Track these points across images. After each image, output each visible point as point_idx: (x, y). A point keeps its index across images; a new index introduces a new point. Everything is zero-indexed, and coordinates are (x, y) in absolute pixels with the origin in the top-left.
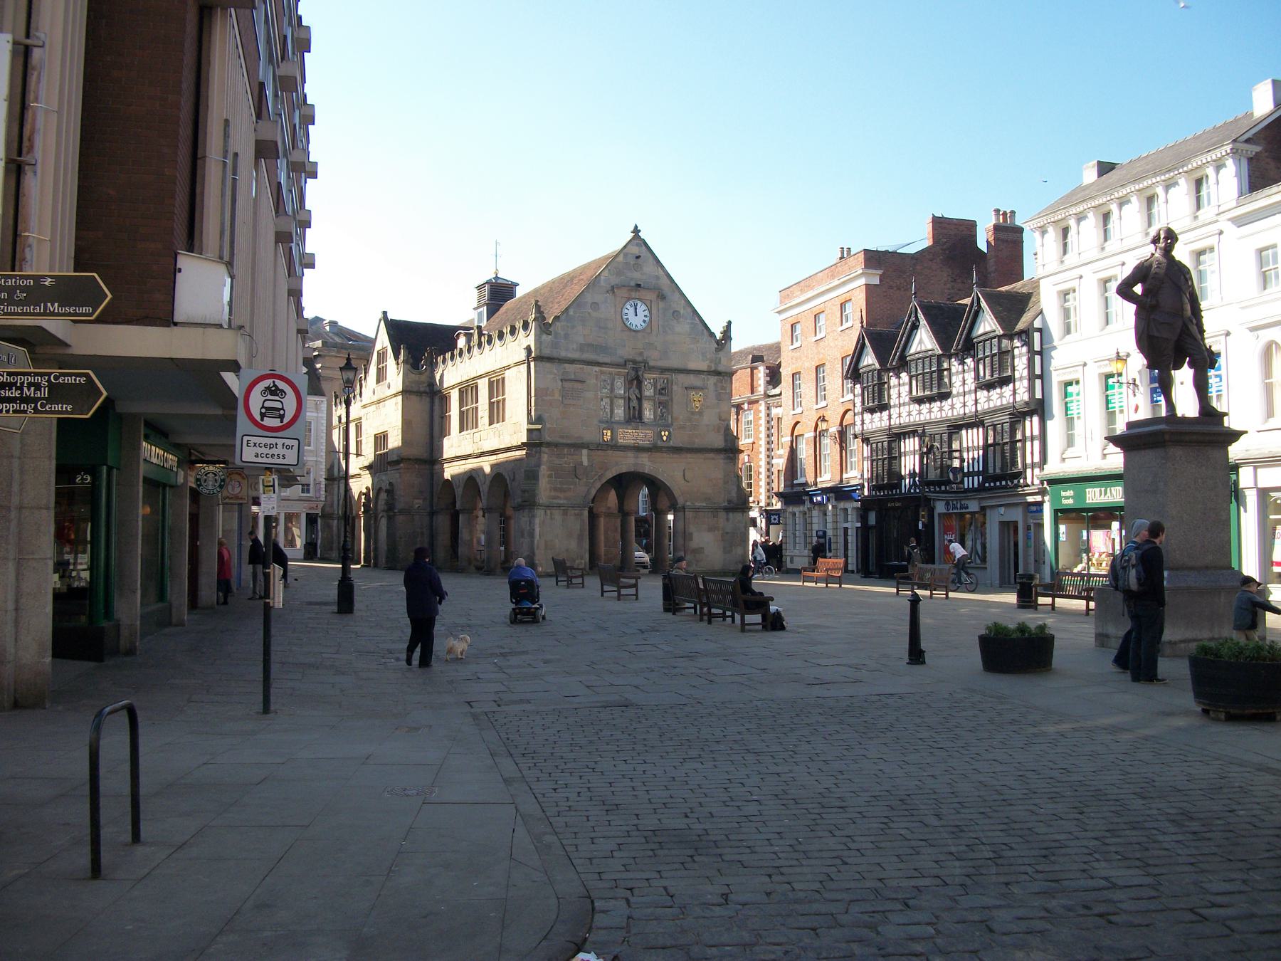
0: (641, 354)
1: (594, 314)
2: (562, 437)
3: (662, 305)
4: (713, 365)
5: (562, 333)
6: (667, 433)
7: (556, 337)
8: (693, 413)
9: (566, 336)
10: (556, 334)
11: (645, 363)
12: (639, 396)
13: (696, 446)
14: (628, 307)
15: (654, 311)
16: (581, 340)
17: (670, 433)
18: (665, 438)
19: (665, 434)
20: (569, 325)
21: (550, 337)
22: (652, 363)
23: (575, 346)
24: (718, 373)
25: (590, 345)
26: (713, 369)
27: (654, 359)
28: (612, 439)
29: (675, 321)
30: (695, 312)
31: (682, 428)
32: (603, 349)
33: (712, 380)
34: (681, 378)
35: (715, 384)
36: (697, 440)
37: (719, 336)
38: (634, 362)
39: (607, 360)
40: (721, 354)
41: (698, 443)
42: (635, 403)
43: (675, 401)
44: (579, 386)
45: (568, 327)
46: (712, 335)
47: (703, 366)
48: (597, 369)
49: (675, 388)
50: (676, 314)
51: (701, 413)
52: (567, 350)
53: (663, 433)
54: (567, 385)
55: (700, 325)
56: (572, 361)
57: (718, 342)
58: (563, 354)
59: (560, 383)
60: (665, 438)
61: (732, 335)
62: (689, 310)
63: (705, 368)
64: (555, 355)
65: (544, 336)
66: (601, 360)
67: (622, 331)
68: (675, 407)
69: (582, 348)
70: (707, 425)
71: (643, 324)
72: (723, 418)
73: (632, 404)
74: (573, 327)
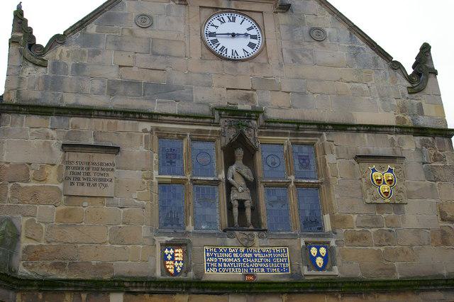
0: (247, 98)
1: (141, 33)
2: (59, 266)
3: (283, 18)
4: (408, 118)
5: (70, 63)
6: (323, 250)
7: (54, 70)
8: (379, 206)
9: (79, 69)
10: (56, 65)
11: (256, 113)
12: (250, 178)
13: (398, 276)
14: (216, 22)
15: (270, 27)
16: (113, 74)
17: (330, 251)
18: (319, 261)
19: (317, 252)
20: (86, 50)
21: (43, 69)
22: (272, 114)
23: (97, 85)
24: (420, 131)
25: (131, 83)
26: (409, 123)
27: (276, 106)
28: (186, 270)
29: (316, 43)
30: (354, 29)
31: (353, 239)
32: (165, 90)
33: (410, 144)
34: (342, 138)
35: (420, 151)
36: (396, 264)
37: (410, 71)
38: (232, 112)
39: (173, 108)
40: (423, 99)
41: (400, 269)
42: (241, 193)
43: (334, 181)
44: (106, 158)
45: (84, 53)
46: (397, 66)
47: (389, 119)
48: (148, 126)
49: (330, 158)
50: (317, 35)
51: (398, 206)
52: (79, 92)
53: (314, 251)
54: (74, 157)
55: (369, 52)
56: (86, 112)
57: (409, 78)
58: (70, 99)
59: (59, 154)
60: (319, 261)
61: (437, 65)
62: (343, 27)
63: (392, 122)
64: (50, 99)
65: (30, 68)
66: (156, 108)
67: (202, 59)
68: (336, 196)
69: (112, 88)
70: (418, 230)
71: (250, 50)
72: (449, 215)
73: (234, 196)
74: (96, 53)
